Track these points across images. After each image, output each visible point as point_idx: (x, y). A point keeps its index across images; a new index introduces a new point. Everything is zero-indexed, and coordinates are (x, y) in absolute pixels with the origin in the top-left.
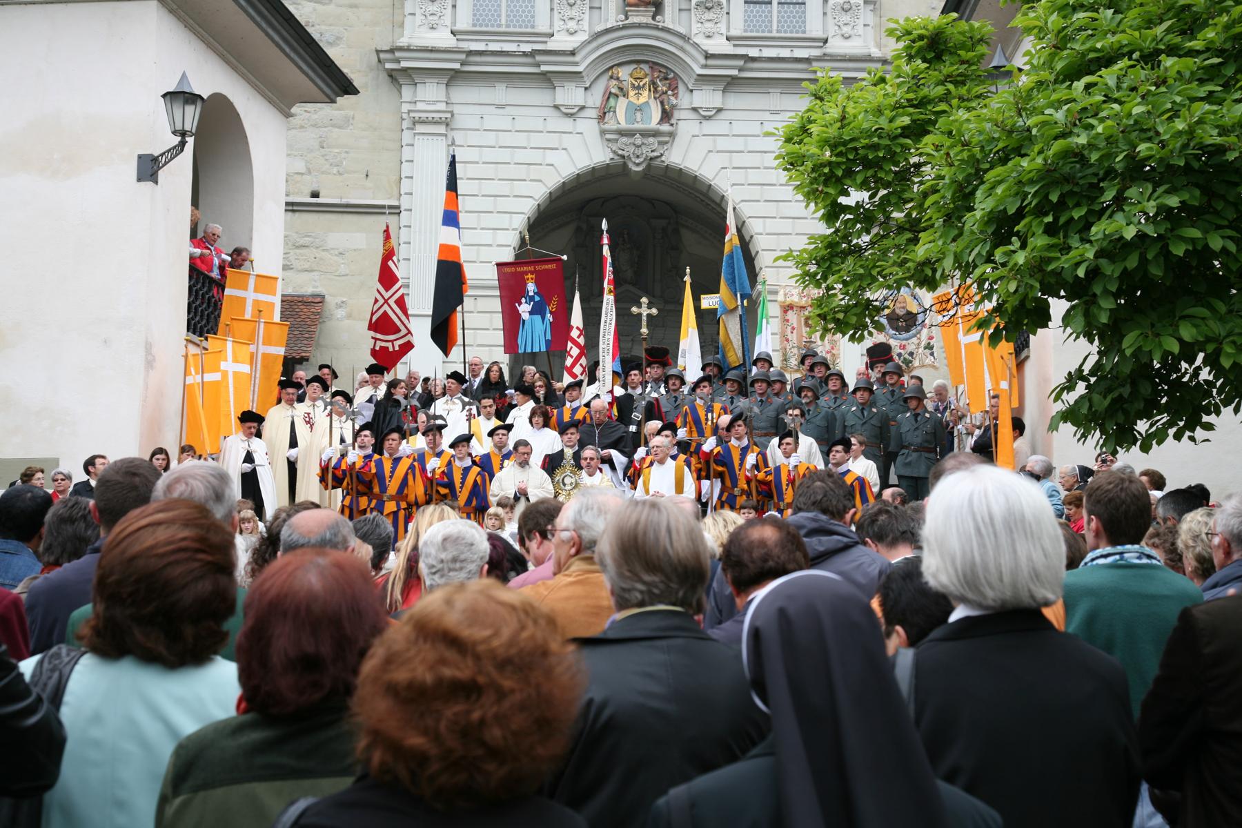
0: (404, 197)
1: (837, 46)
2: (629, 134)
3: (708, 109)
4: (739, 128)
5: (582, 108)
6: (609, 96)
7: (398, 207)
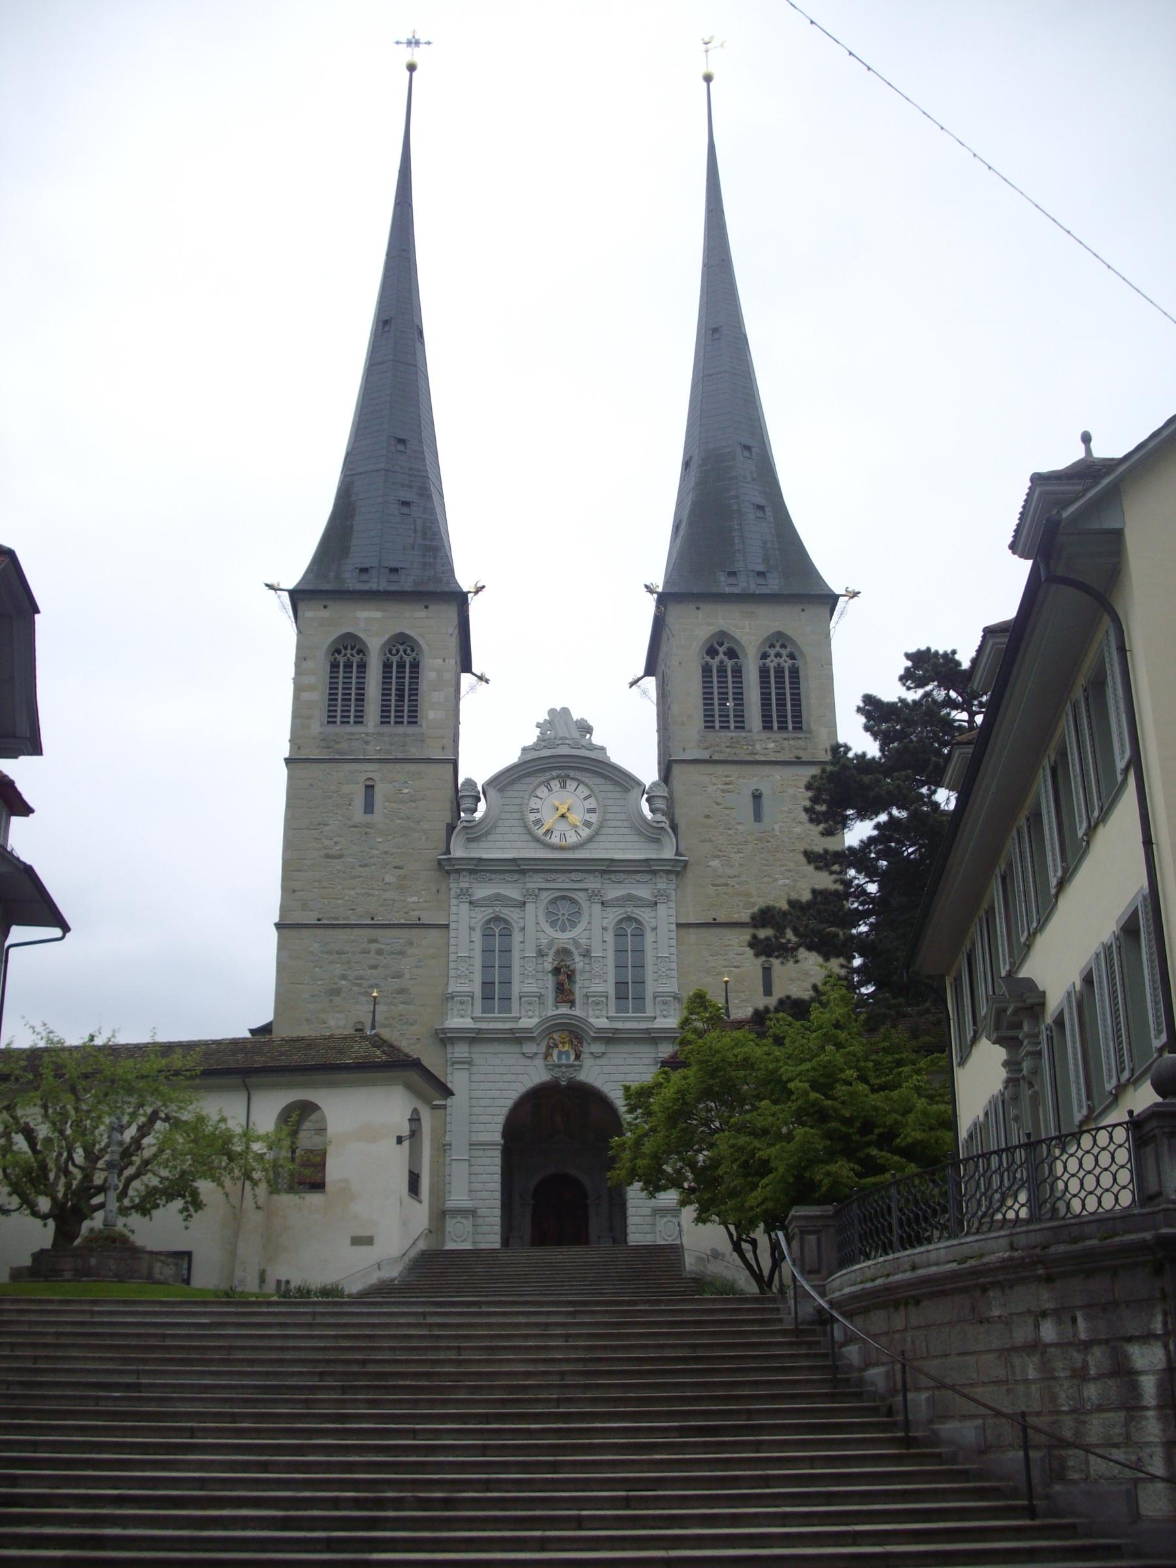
2: (560, 1066)
4: (615, 1062)
6: (549, 1047)
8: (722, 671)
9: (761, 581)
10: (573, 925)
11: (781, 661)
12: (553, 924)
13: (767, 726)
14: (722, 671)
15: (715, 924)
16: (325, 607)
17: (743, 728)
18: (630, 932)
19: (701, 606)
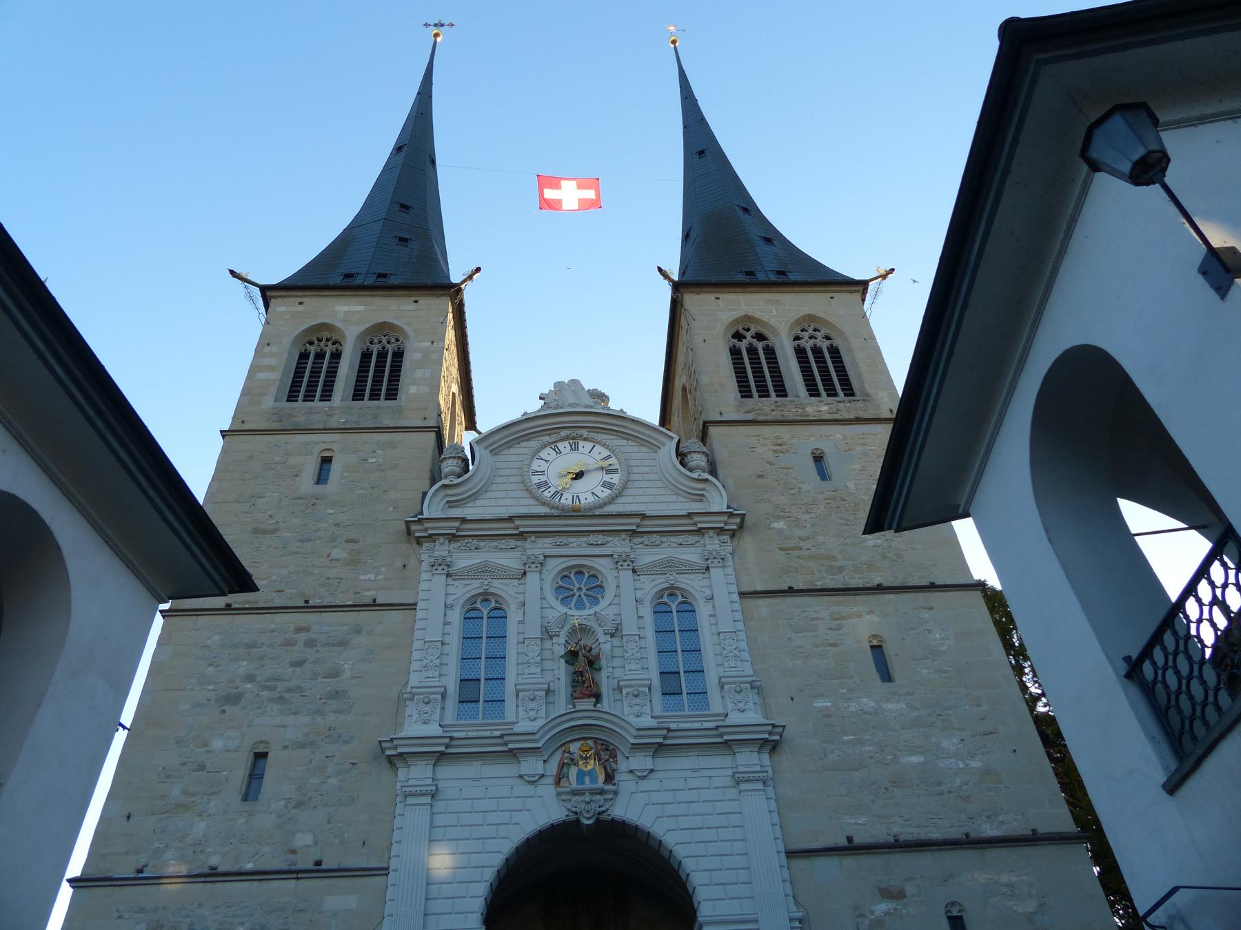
0: (393, 860)
1: (735, 718)
3: (642, 771)
5: (542, 776)
6: (562, 765)
7: (387, 869)
8: (752, 351)
10: (595, 601)
12: (565, 601)
14: (752, 351)
15: (791, 591)
17: (786, 396)
18: (673, 608)
19: (720, 296)
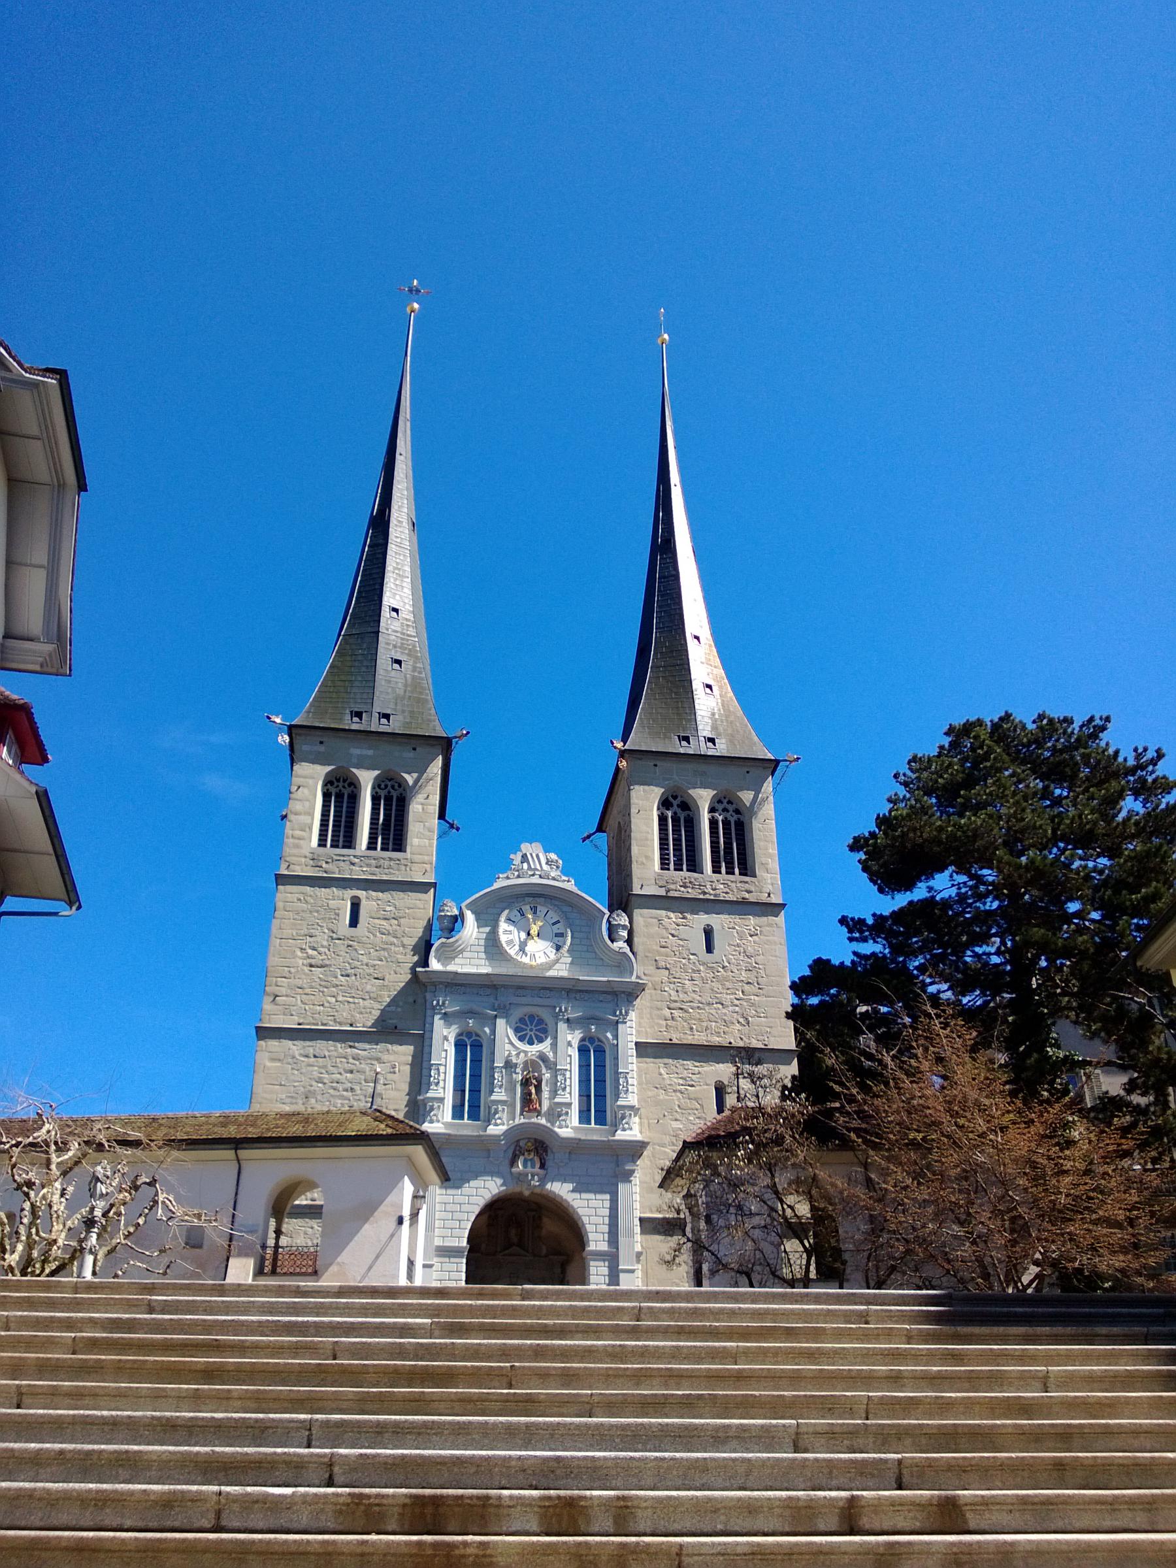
8: (676, 820)
9: (710, 744)
11: (728, 815)
13: (716, 870)
16: (321, 743)
